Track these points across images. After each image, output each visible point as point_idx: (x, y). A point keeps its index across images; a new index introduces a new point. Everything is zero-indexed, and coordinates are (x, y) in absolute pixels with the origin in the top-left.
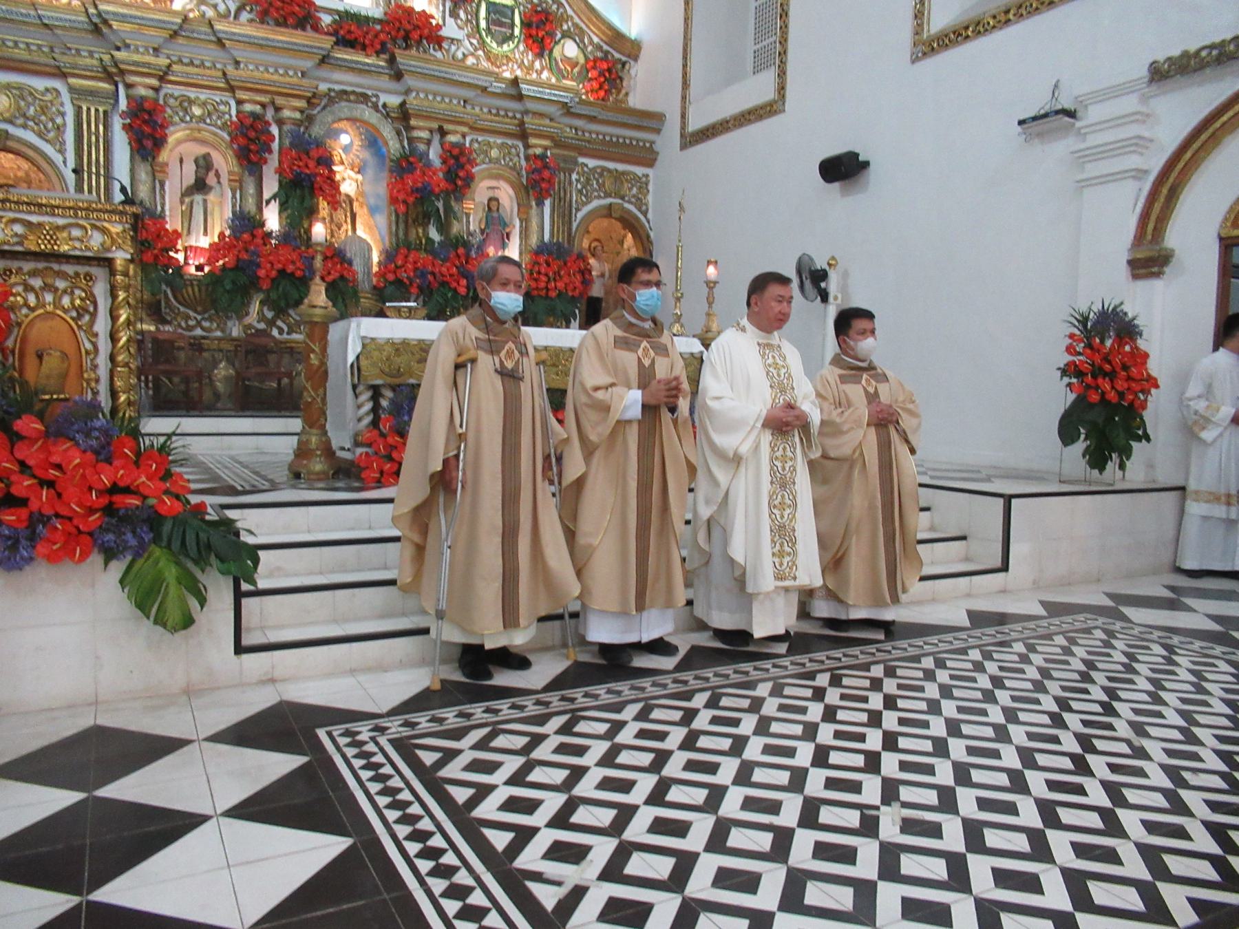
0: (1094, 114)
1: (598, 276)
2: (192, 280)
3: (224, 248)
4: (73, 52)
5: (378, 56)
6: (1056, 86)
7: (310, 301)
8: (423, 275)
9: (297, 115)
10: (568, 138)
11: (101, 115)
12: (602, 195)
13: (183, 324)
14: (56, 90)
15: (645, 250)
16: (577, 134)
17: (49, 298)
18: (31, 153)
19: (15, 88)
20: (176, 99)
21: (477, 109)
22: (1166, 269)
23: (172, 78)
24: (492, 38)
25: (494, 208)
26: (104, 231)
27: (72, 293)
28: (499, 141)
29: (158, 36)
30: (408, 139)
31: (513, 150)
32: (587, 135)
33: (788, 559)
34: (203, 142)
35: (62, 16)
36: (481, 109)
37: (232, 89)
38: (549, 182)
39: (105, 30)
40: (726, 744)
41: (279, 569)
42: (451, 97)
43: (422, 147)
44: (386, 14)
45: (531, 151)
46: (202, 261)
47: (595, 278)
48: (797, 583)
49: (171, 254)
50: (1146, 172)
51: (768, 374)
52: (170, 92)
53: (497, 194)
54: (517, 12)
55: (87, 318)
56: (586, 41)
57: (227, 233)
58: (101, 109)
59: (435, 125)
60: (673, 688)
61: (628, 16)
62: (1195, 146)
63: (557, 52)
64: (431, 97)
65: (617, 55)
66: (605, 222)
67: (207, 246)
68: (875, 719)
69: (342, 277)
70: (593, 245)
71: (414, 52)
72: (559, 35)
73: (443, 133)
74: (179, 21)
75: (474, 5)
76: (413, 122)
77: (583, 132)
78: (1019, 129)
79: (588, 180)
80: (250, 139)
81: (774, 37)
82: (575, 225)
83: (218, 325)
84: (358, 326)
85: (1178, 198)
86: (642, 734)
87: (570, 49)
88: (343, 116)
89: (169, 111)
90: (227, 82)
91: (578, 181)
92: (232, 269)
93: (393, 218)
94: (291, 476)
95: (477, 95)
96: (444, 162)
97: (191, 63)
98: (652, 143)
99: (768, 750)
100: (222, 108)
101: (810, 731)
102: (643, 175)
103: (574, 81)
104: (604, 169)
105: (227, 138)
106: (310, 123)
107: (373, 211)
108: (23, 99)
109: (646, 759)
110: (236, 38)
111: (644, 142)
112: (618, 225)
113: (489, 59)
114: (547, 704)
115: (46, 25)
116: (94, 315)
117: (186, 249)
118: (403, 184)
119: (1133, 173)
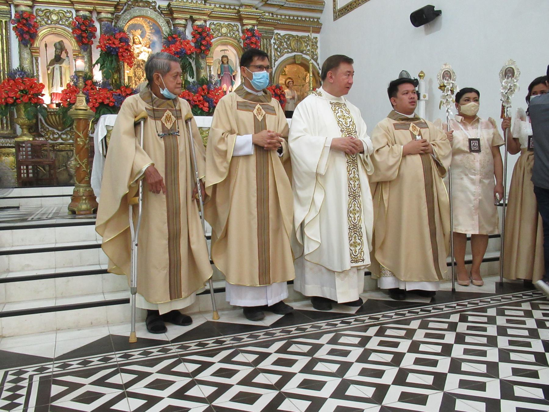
1: (291, 99)
2: (55, 113)
3: (70, 93)
7: (76, 106)
9: (109, 16)
12: (290, 51)
13: (51, 137)
20: (43, 11)
21: (213, 6)
25: (225, 62)
28: (226, 23)
30: (173, 25)
34: (58, 34)
36: (215, 5)
41: (28, 266)
43: (181, 29)
45: (245, 28)
47: (289, 101)
48: (365, 264)
49: (40, 97)
52: (39, 8)
53: (227, 53)
57: (72, 84)
59: (188, 16)
66: (295, 68)
67: (60, 92)
73: (193, 20)
76: (175, 15)
77: (277, 15)
79: (281, 42)
80: (82, 31)
83: (71, 137)
84: (105, 120)
89: (39, 18)
91: (275, 43)
94: (70, 213)
96: (194, 37)
100: (68, 14)
102: (314, 38)
105: (71, 31)
106: (118, 20)
111: (313, 18)
117: (51, 95)
118: (170, 50)
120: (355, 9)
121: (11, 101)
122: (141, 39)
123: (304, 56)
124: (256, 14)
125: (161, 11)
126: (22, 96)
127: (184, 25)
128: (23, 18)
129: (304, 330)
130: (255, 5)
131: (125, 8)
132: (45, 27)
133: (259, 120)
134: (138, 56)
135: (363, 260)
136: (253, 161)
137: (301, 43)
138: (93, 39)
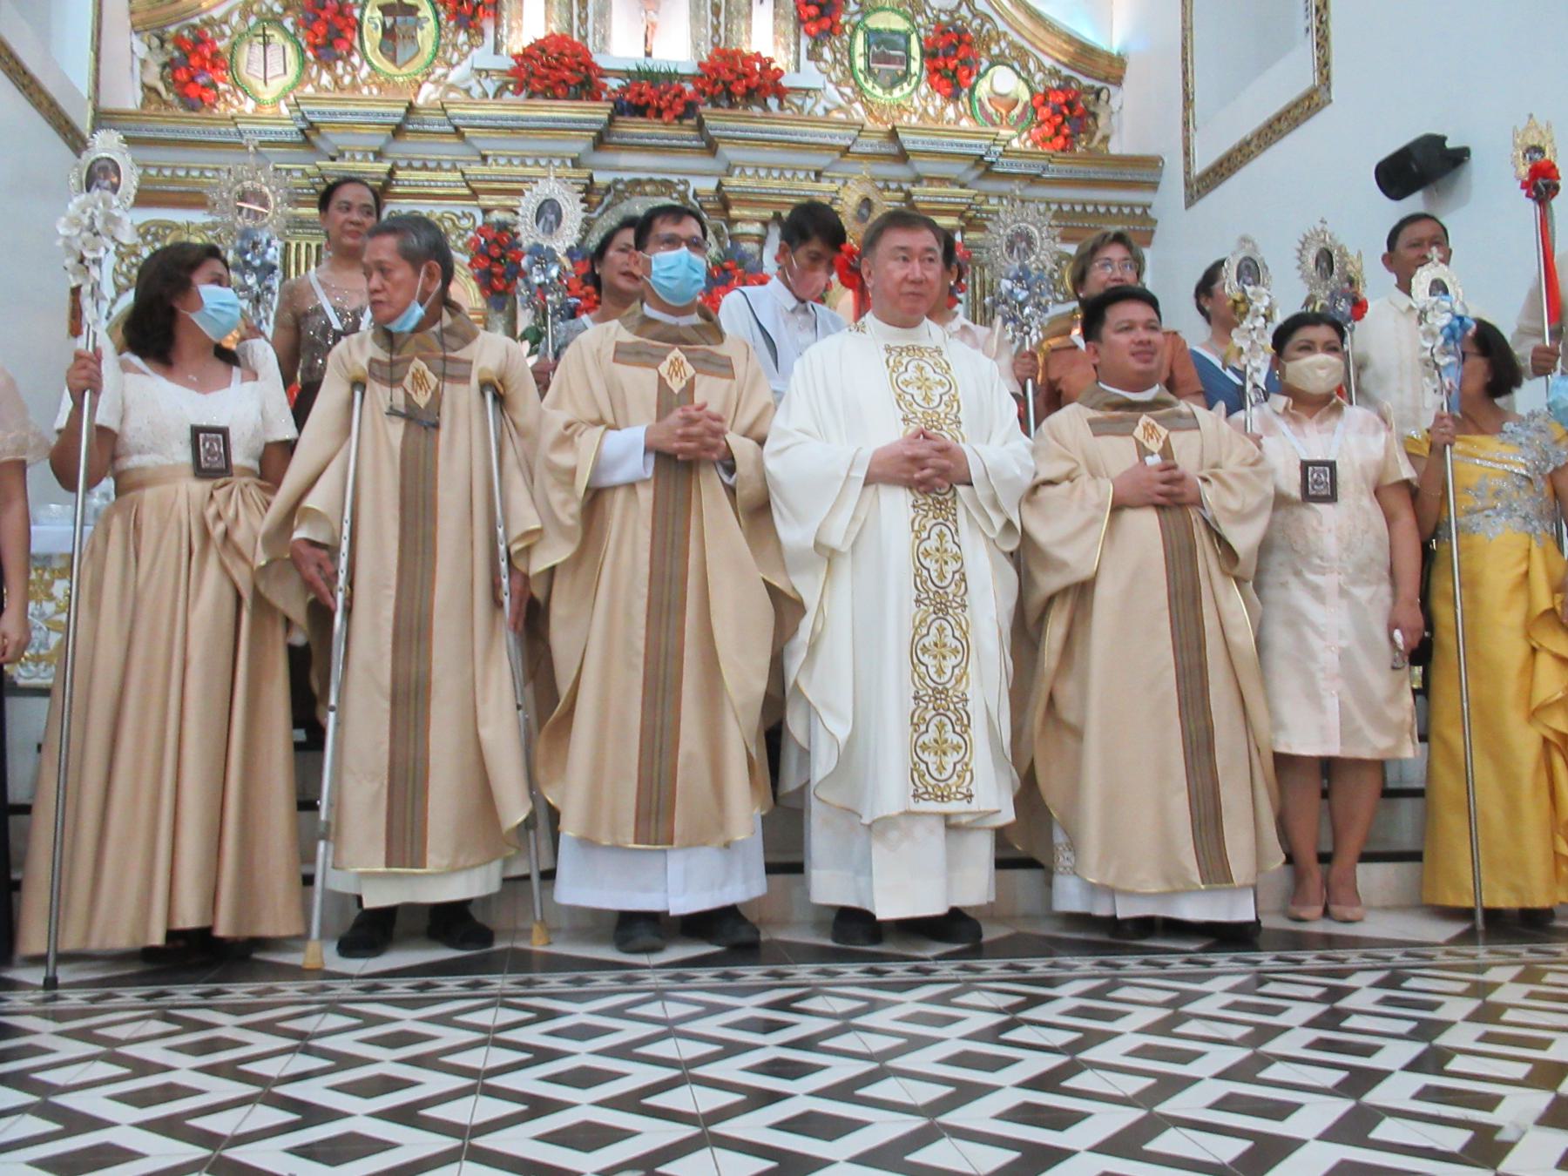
5: (680, 123)
12: (1060, 298)
23: (398, 190)
24: (875, 81)
37: (475, 194)
39: (313, 138)
42: (795, 170)
43: (749, 247)
44: (700, 65)
48: (975, 806)
54: (914, 38)
56: (1032, 66)
59: (769, 214)
63: (983, 89)
64: (762, 173)
65: (1086, 82)
71: (740, 111)
72: (985, 63)
74: (403, 110)
75: (846, 37)
80: (492, 259)
87: (1001, 82)
97: (425, 168)
98: (1146, 207)
100: (465, 223)
103: (1012, 128)
110: (477, 122)
111: (1132, 206)
120: (1239, 169)
124: (958, 200)
125: (700, 203)
127: (758, 235)
130: (955, 176)
131: (607, 200)
133: (672, 391)
135: (969, 797)
136: (646, 495)
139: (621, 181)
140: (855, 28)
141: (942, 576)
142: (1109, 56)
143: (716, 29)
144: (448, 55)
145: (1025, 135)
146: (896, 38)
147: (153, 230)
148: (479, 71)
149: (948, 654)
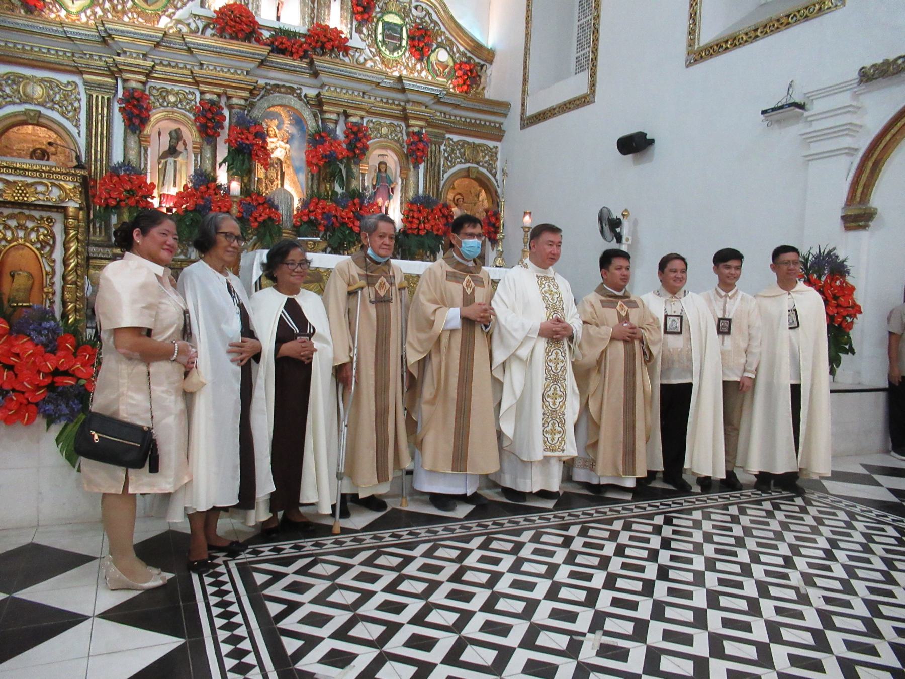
0: (817, 106)
3: (186, 196)
4: (88, 56)
5: (301, 61)
6: (790, 85)
8: (328, 218)
9: (242, 102)
10: (439, 120)
11: (106, 101)
12: (463, 161)
14: (74, 82)
15: (493, 201)
16: (445, 117)
17: (21, 234)
18: (55, 127)
19: (46, 81)
20: (158, 90)
21: (372, 98)
22: (871, 224)
23: (155, 75)
25: (383, 170)
26: (60, 187)
27: (38, 231)
28: (388, 122)
29: (145, 46)
31: (398, 129)
32: (453, 118)
33: (559, 435)
34: (176, 121)
35: (81, 31)
37: (197, 83)
38: (423, 151)
39: (110, 42)
40: (542, 569)
42: (354, 90)
43: (331, 125)
44: (309, 30)
45: (411, 129)
46: (172, 204)
48: (565, 454)
49: (149, 200)
50: (856, 150)
51: (544, 298)
52: (153, 85)
53: (385, 160)
54: (404, 28)
55: (48, 248)
57: (190, 185)
58: (106, 97)
59: (341, 110)
60: (459, 532)
61: (486, 32)
62: (894, 131)
63: (433, 58)
64: (339, 90)
65: (477, 60)
66: (466, 181)
67: (175, 194)
68: (653, 555)
69: (270, 218)
70: (457, 197)
71: (328, 58)
72: (435, 46)
73: (347, 115)
74: (161, 35)
76: (325, 108)
77: (450, 115)
78: (762, 117)
79: (453, 150)
81: (588, 49)
82: (442, 183)
83: (182, 251)
85: (880, 170)
86: (482, 559)
87: (442, 56)
88: (275, 103)
89: (152, 98)
90: (194, 78)
92: (191, 211)
93: (310, 176)
95: (372, 89)
96: (347, 136)
97: (169, 65)
98: (501, 124)
99: (573, 575)
100: (190, 96)
101: (604, 563)
103: (443, 77)
104: (465, 142)
105: (193, 118)
106: (252, 108)
107: (296, 171)
108: (52, 89)
109: (484, 578)
111: (495, 123)
112: (475, 184)
113: (383, 63)
114: (360, 541)
115: (68, 37)
116: (53, 247)
117: (160, 196)
118: (317, 152)
119: (847, 151)
121: (113, 203)
122: (277, 131)
123: (480, 169)
125: (308, 101)
126: (128, 198)
128: (134, 97)
129: (502, 525)
131: (263, 92)
132: (158, 110)
134: (272, 153)
137: (478, 152)
138: (219, 130)
139: (269, 84)
140: (378, 20)
141: (556, 369)
142: (487, 50)
143: (313, 10)
144: (176, 2)
145: (450, 82)
146: (396, 27)
147: (12, 78)
148: (195, 15)
149: (557, 397)
